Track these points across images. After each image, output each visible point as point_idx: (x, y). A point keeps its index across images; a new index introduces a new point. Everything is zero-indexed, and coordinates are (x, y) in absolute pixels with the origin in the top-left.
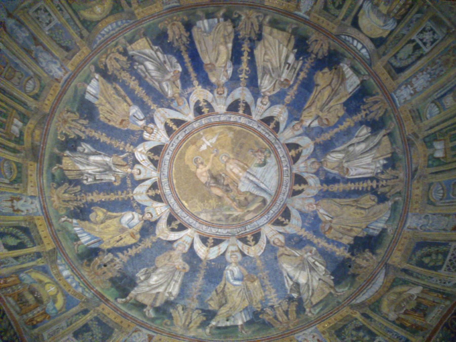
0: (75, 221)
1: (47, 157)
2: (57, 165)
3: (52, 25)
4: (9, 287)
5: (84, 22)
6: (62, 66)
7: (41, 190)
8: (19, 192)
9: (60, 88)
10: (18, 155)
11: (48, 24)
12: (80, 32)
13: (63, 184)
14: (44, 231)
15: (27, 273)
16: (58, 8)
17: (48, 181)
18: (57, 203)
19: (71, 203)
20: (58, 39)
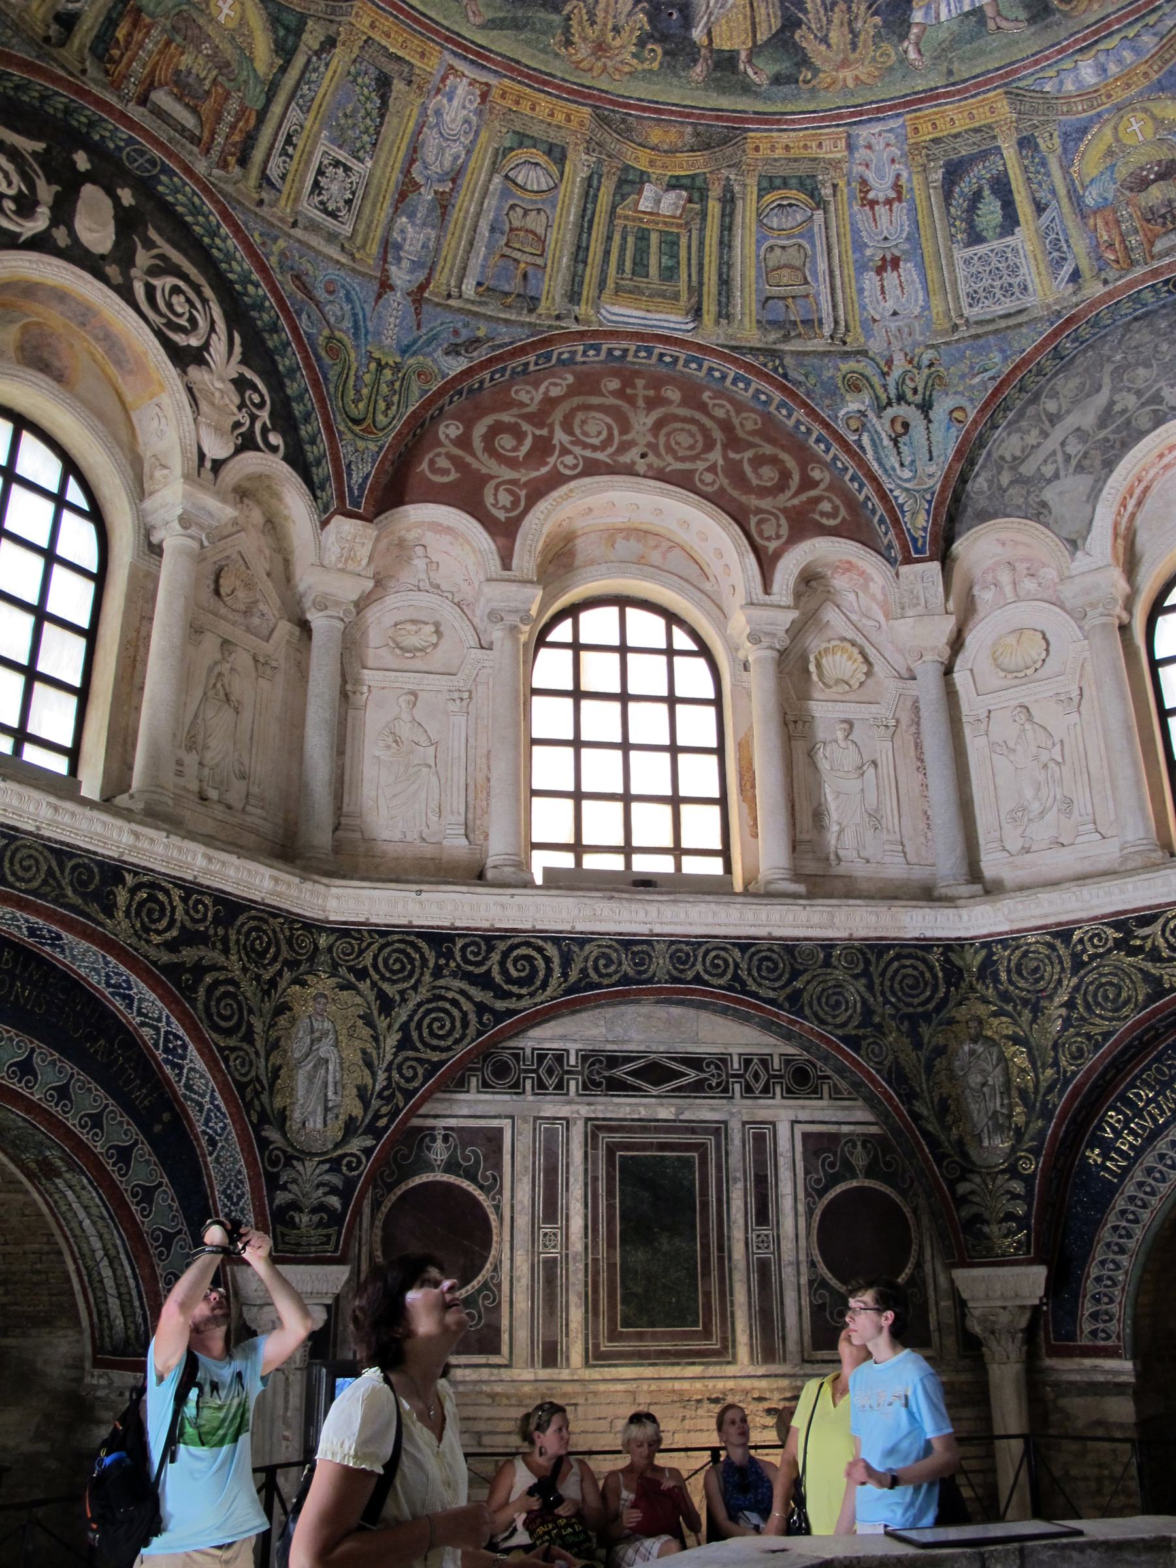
0: (918, 16)
1: (725, 102)
2: (742, 67)
3: (342, 155)
4: (1123, 241)
5: (285, 51)
6: (438, 91)
7: (831, 117)
8: (842, 184)
9: (506, 81)
10: (737, 188)
11: (347, 169)
12: (318, 53)
13: (799, 49)
14: (954, 118)
15: (1085, 188)
16: (290, 150)
17: (796, 97)
18: (862, 71)
19: (860, 24)
20: (368, 121)
